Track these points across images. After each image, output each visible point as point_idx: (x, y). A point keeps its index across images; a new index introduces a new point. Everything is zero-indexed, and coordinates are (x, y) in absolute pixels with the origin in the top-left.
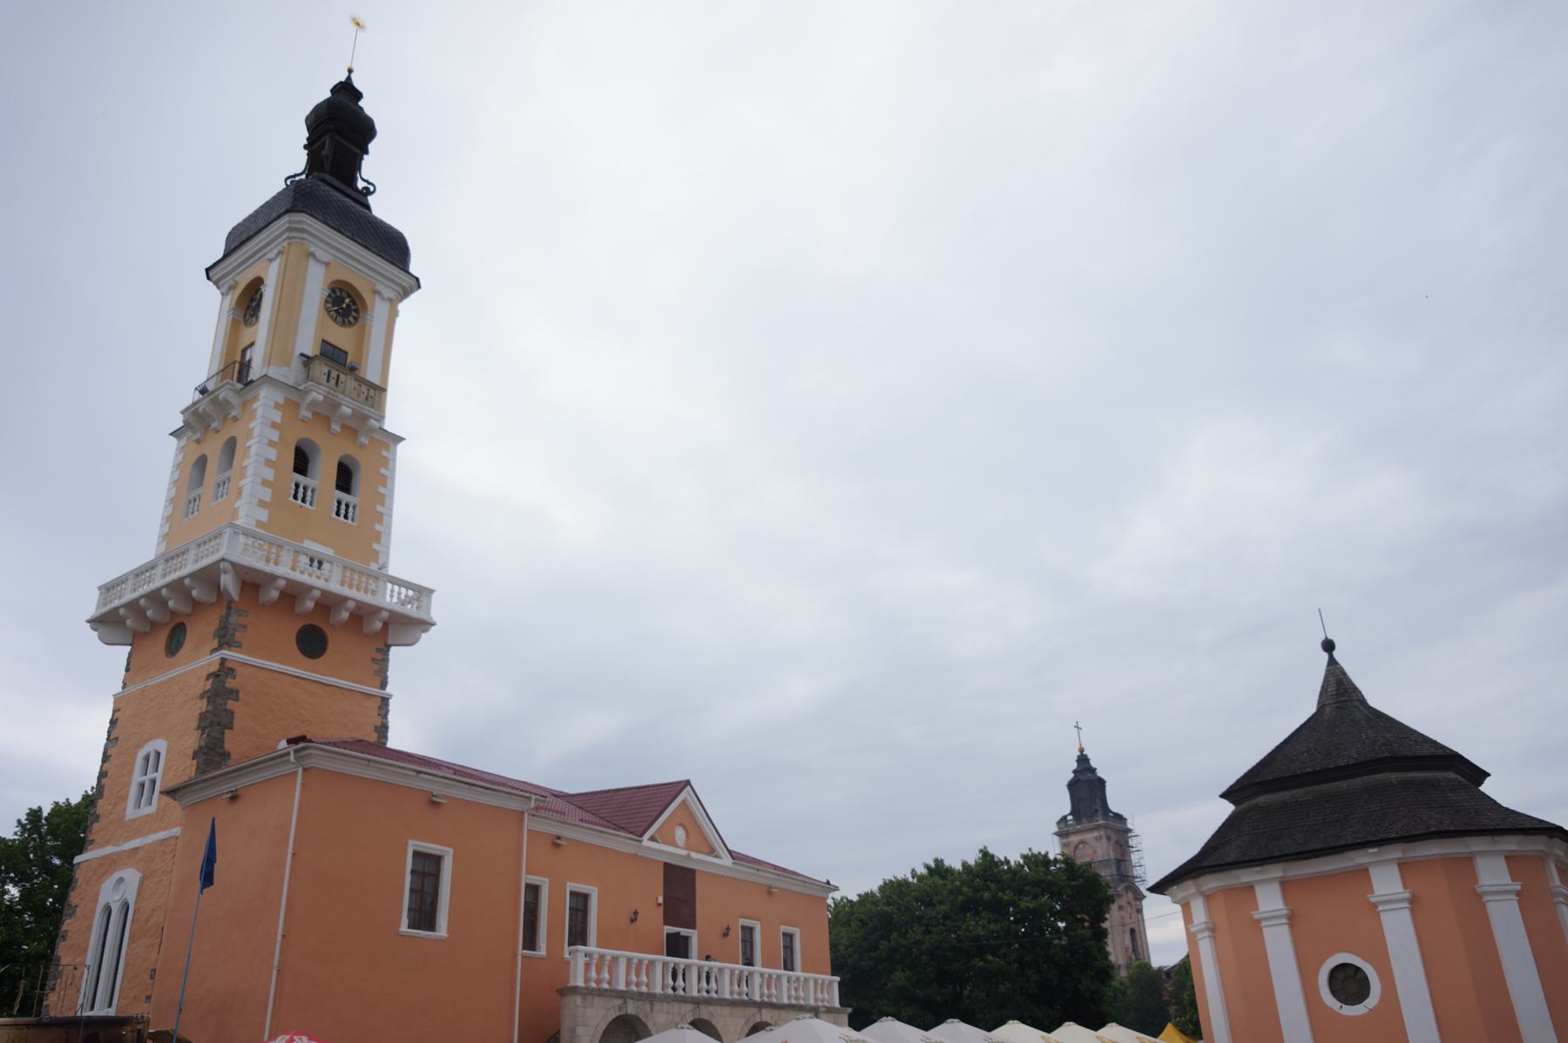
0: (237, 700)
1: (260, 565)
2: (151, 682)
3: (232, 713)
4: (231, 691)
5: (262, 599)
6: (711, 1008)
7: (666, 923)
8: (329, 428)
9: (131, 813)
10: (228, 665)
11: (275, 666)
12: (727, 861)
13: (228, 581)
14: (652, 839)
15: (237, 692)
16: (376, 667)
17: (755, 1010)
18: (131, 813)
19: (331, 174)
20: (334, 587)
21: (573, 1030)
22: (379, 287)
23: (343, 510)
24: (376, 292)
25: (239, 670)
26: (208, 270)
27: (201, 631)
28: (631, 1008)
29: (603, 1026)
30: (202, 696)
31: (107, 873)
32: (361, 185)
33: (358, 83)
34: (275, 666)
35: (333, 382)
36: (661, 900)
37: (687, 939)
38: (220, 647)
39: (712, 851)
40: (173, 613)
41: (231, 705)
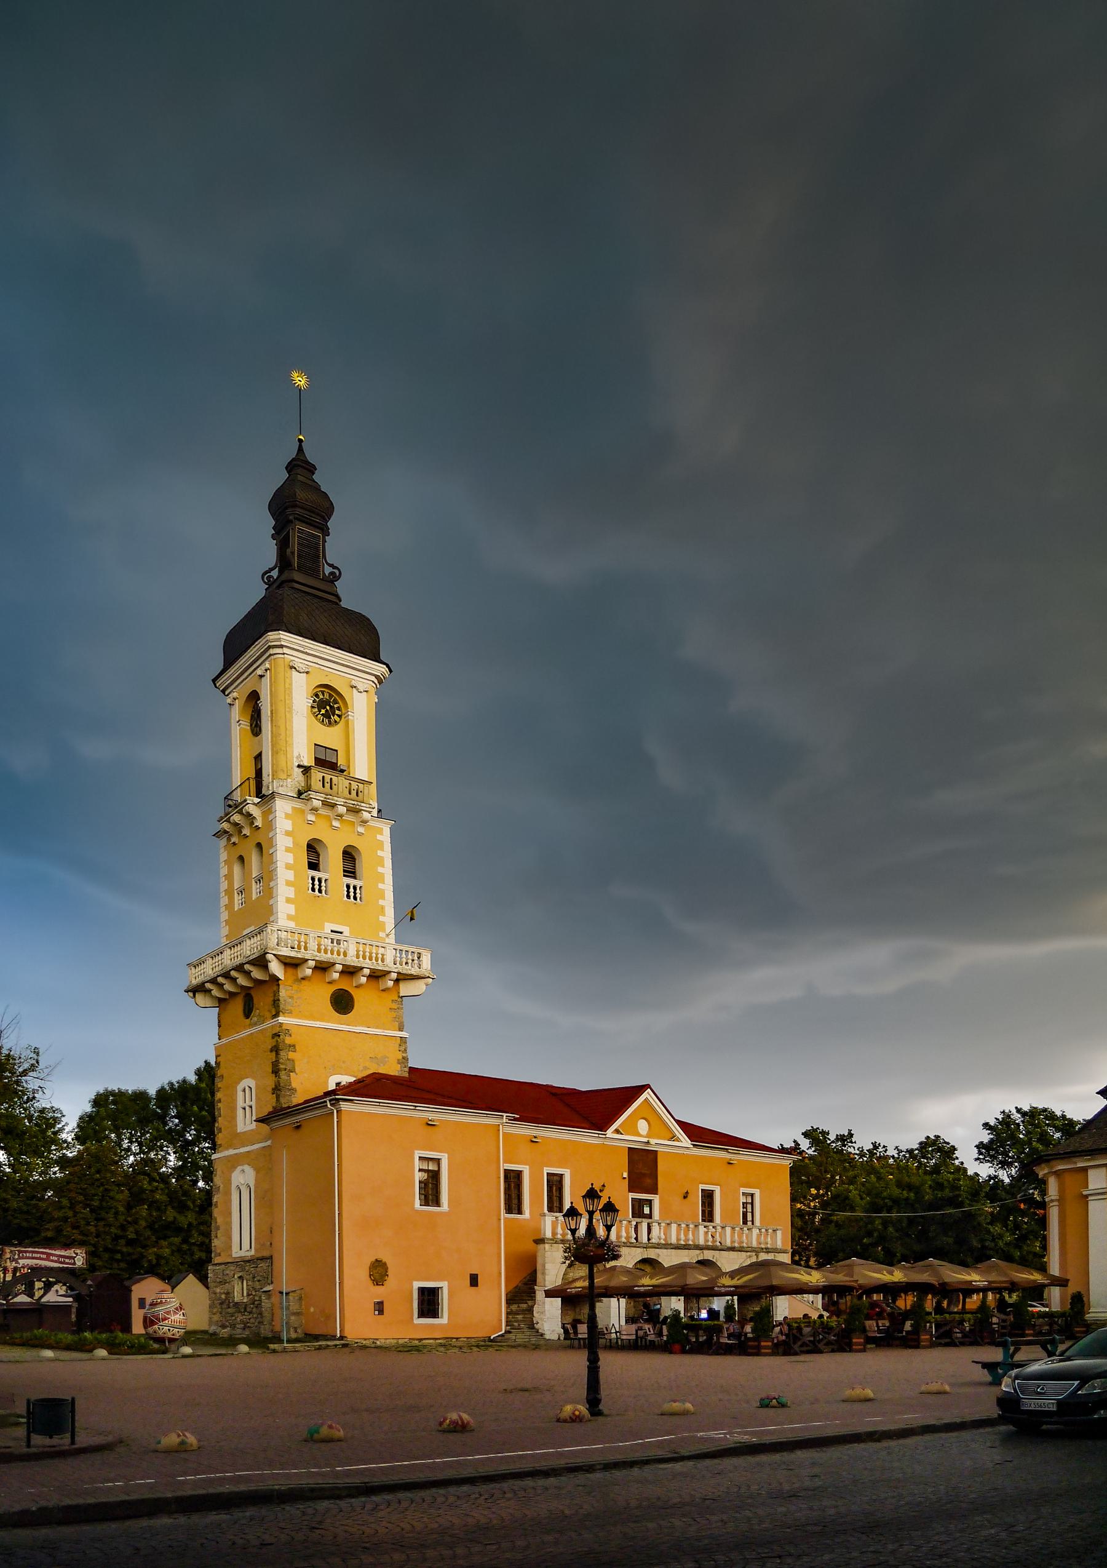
1: (293, 954)
2: (237, 1036)
4: (290, 1046)
7: (630, 1191)
9: (241, 1128)
10: (284, 1027)
11: (318, 1024)
12: (686, 1142)
13: (275, 968)
15: (294, 1046)
17: (698, 1252)
18: (241, 1128)
19: (300, 569)
21: (544, 1266)
25: (293, 1031)
27: (262, 1002)
30: (271, 1051)
31: (234, 1168)
34: (318, 1024)
35: (327, 786)
36: (625, 1175)
37: (650, 1203)
38: (276, 1015)
40: (242, 987)
41: (291, 1055)
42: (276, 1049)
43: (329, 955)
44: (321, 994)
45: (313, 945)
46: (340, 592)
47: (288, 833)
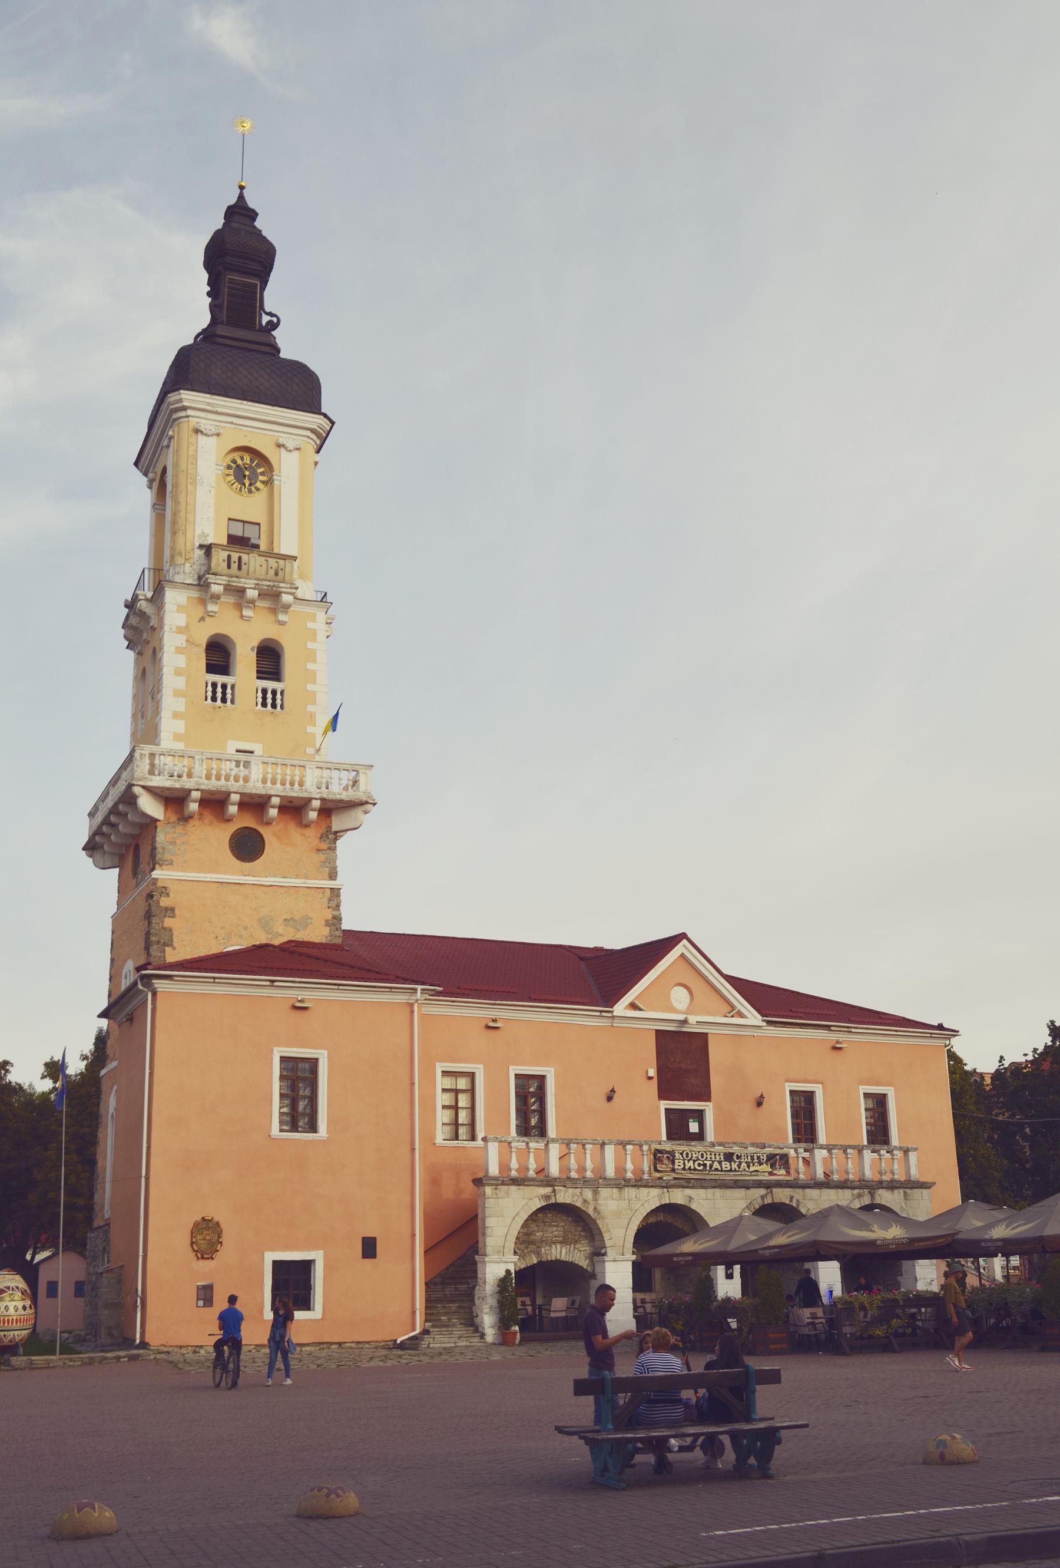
0: (174, 916)
1: (168, 784)
3: (171, 930)
4: (166, 909)
5: (186, 814)
6: (688, 1192)
7: (661, 1097)
8: (242, 616)
10: (159, 884)
12: (753, 1017)
14: (633, 1006)
15: (173, 909)
16: (322, 857)
17: (762, 1191)
20: (256, 787)
22: (281, 441)
23: (270, 700)
24: (279, 446)
26: (136, 464)
28: (565, 1196)
29: (525, 1216)
32: (265, 319)
33: (251, 202)
35: (234, 566)
36: (652, 1072)
39: (733, 1011)
41: (168, 922)
42: (148, 916)
43: (223, 782)
44: (220, 836)
45: (200, 770)
46: (280, 342)
47: (180, 630)
